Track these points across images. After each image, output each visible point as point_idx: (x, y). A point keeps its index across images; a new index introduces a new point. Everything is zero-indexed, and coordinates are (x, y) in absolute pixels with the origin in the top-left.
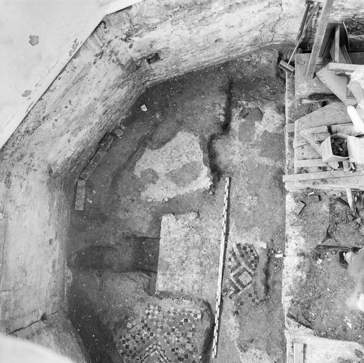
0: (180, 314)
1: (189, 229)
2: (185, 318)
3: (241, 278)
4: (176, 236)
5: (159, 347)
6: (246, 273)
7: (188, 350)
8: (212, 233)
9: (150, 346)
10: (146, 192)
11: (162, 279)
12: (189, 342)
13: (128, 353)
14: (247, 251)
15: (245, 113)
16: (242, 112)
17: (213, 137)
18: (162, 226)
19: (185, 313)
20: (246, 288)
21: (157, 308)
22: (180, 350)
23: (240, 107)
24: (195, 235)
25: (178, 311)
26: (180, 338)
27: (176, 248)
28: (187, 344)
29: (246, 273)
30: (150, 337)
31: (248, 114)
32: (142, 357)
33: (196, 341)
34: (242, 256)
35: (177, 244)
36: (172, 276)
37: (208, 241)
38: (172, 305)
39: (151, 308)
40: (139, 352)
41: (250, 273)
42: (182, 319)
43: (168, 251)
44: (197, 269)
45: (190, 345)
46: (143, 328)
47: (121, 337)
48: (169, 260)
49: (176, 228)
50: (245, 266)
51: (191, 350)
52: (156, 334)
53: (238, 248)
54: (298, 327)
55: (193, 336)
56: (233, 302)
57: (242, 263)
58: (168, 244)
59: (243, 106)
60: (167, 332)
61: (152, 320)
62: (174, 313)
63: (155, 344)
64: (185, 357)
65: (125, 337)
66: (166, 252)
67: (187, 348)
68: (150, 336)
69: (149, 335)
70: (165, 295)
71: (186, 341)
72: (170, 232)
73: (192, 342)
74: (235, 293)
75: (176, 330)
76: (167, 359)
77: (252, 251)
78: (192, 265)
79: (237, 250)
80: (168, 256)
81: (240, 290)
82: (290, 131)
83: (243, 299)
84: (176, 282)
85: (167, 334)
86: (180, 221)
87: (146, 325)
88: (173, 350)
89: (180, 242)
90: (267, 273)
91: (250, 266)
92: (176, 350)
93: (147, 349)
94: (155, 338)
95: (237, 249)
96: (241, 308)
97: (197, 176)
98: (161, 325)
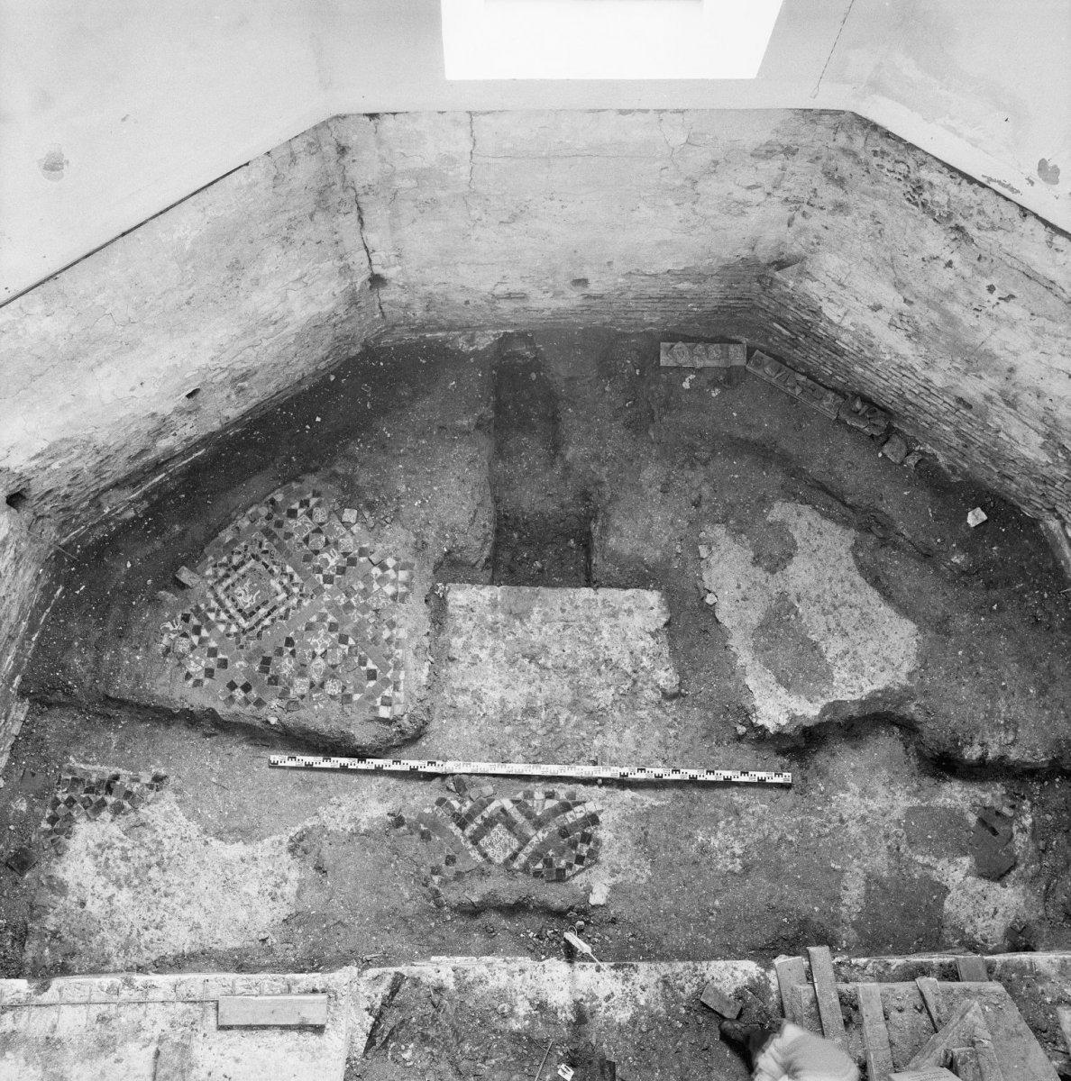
0: (388, 657)
1: (629, 670)
2: (378, 672)
3: (499, 831)
4: (605, 634)
5: (294, 601)
6: (516, 844)
7: (291, 684)
8: (620, 741)
9: (296, 578)
10: (728, 538)
11: (480, 599)
12: (312, 685)
13: (275, 516)
14: (579, 845)
15: (995, 825)
16: (998, 813)
17: (908, 728)
18: (630, 592)
19: (391, 671)
20: (470, 846)
21: (402, 589)
22: (290, 663)
23: (1013, 807)
24: (612, 690)
25: (397, 651)
27: (571, 637)
28: (307, 680)
29: (516, 844)
30: (321, 576)
31: (994, 832)
32: (268, 555)
33: (316, 707)
34: (564, 832)
35: (584, 638)
36: (492, 629)
37: (598, 728)
38: (412, 634)
39: (400, 572)
40: (280, 547)
41: (514, 856)
42: (374, 663)
43: (561, 614)
44: (516, 700)
45: (305, 689)
46: (345, 554)
47: (316, 494)
48: (536, 616)
49: (629, 633)
50: (534, 840)
51: (291, 691)
52: (331, 593)
53: (584, 818)
54: (367, 1009)
55: (331, 696)
56: (427, 811)
57: (544, 832)
59: (1014, 817)
60: (336, 621)
61: (367, 578)
62: (389, 641)
63: (304, 591)
64: (273, 677)
65: (318, 505)
66: (557, 609)
67: (298, 681)
68: (324, 576)
69: (325, 572)
70: (439, 611)
71: (317, 678)
72: (614, 615)
74: (453, 816)
75: (345, 646)
76: (265, 627)
77: (580, 860)
78: (526, 685)
79: (580, 816)
80: (545, 614)
81: (463, 829)
82: (961, 968)
83: (438, 839)
84: (474, 640)
86: (649, 642)
87: (352, 562)
88: (289, 642)
89: (590, 645)
90: (516, 909)
91: (536, 856)
92: (290, 649)
93: (289, 569)
94: (319, 590)
95: (582, 815)
96: (412, 834)
97: (788, 686)
98: (355, 604)
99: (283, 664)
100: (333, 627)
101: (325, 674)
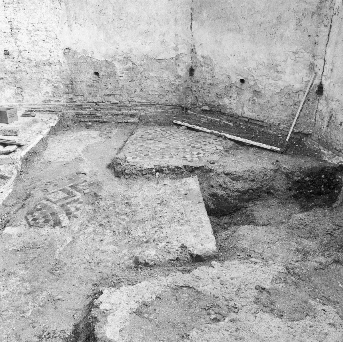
10: (276, 273)
58: (191, 217)
66: (192, 209)
81: (69, 187)
86: (177, 245)
97: (139, 313)
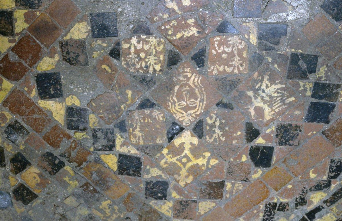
2: (34, 93)
7: (256, 61)
12: (199, 59)
22: (259, 111)
26: (178, 117)
42: (47, 115)
45: (218, 47)
51: (254, 40)
55: (149, 33)
60: (152, 203)
64: (304, 76)
67: (237, 67)
73: (194, 31)
75: (124, 150)
76: (319, 187)
85: (164, 197)
88: (262, 157)
92: (260, 141)
99: (277, 107)
100: (158, 190)
101: (169, 87)
